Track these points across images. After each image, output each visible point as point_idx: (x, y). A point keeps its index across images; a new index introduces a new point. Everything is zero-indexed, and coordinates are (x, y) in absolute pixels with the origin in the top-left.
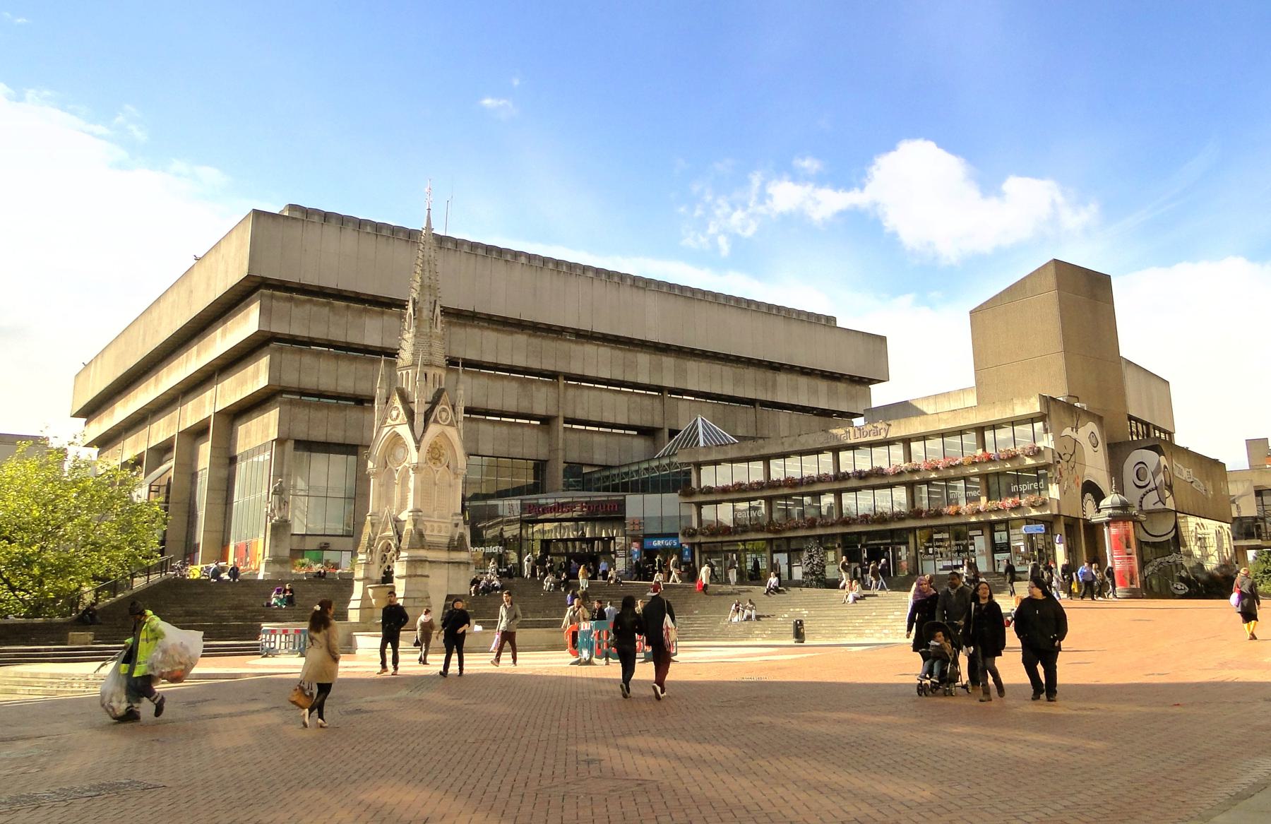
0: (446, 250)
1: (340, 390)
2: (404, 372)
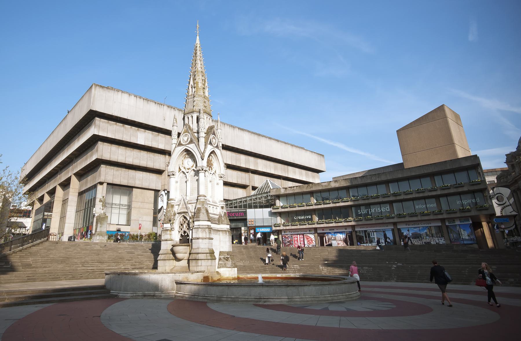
0: (170, 108)
1: (127, 162)
2: (190, 116)
